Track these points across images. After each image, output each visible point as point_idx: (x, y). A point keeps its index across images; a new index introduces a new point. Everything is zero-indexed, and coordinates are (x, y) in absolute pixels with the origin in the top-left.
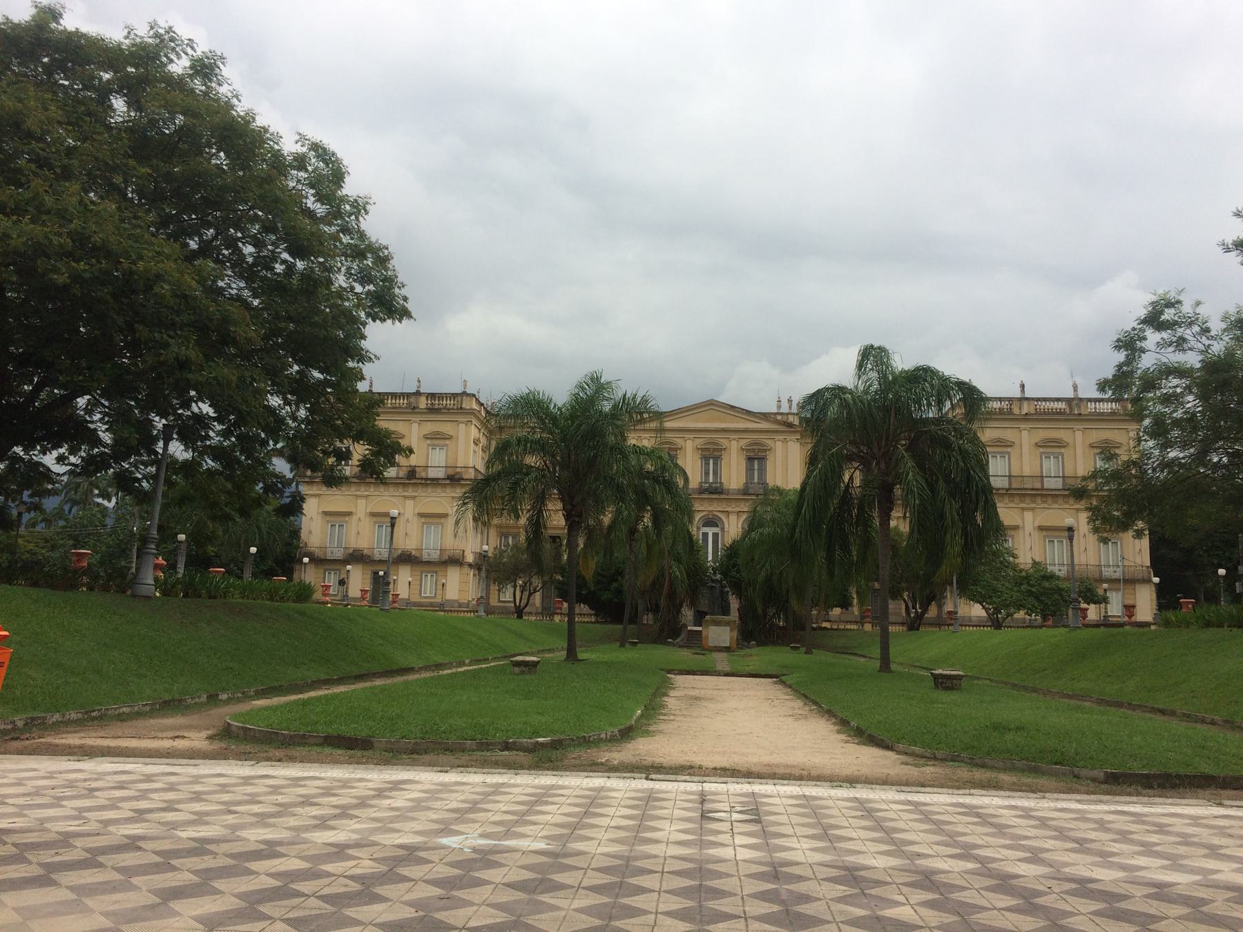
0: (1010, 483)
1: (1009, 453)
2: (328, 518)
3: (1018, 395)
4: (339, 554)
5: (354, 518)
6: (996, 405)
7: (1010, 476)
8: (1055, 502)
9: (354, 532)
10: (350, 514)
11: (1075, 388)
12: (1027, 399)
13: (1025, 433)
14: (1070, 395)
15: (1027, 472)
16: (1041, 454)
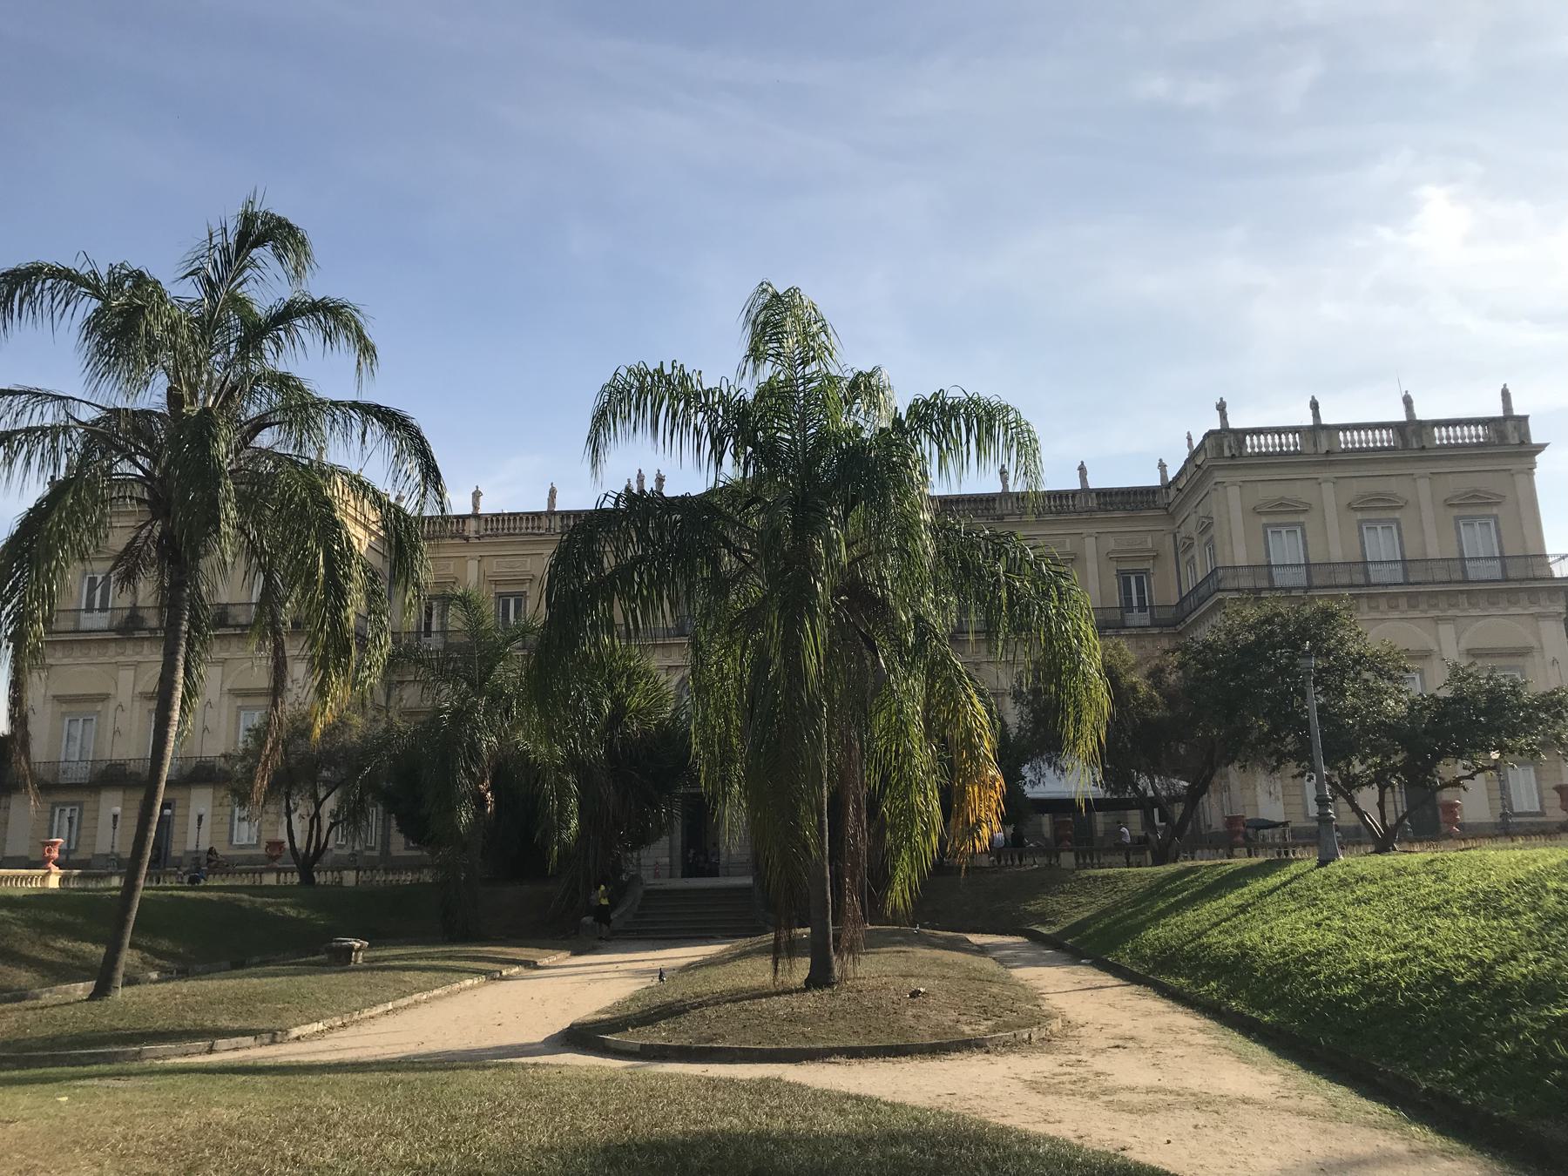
0: (1309, 577)
1: (1301, 525)
2: (64, 708)
3: (1309, 422)
4: (80, 773)
5: (112, 705)
6: (1268, 443)
7: (1307, 564)
8: (1396, 608)
9: (110, 728)
10: (104, 698)
11: (1408, 402)
12: (1327, 427)
13: (1327, 489)
14: (1402, 417)
15: (1337, 555)
16: (1360, 523)
